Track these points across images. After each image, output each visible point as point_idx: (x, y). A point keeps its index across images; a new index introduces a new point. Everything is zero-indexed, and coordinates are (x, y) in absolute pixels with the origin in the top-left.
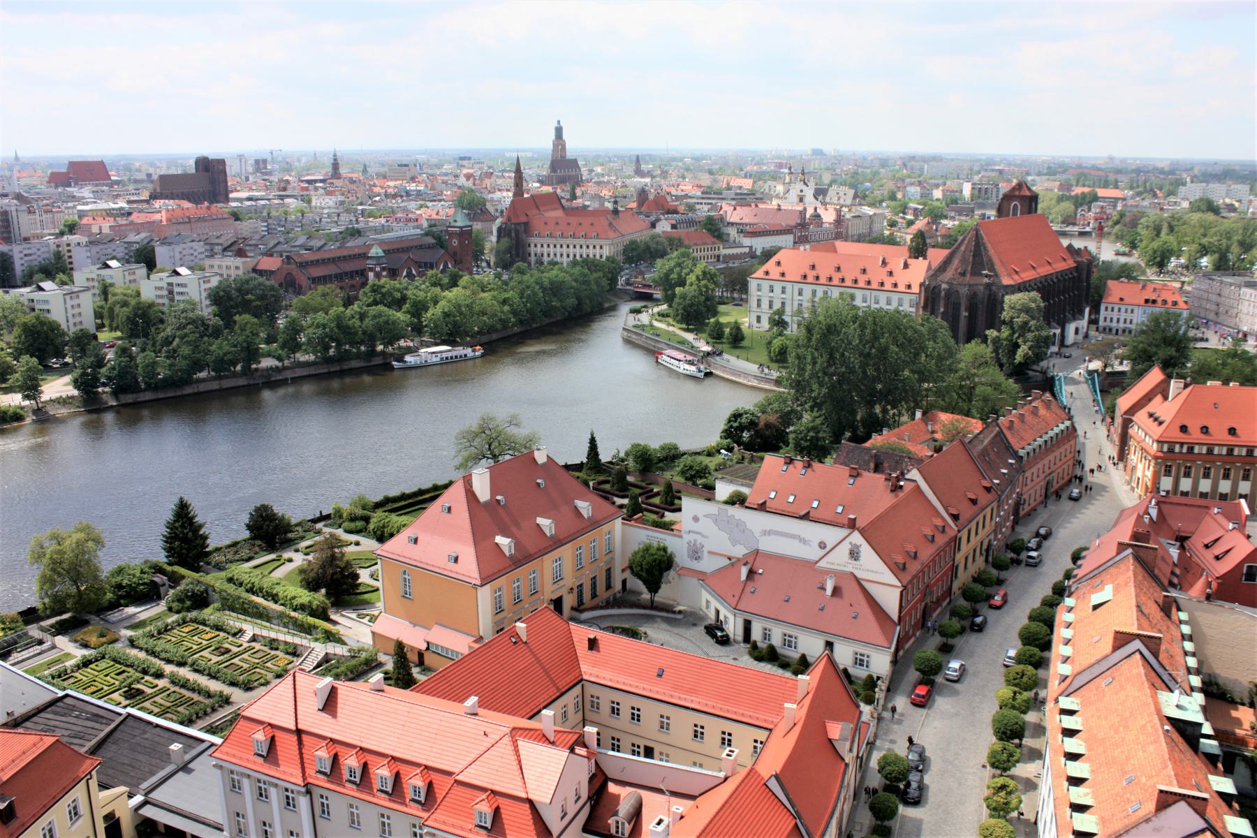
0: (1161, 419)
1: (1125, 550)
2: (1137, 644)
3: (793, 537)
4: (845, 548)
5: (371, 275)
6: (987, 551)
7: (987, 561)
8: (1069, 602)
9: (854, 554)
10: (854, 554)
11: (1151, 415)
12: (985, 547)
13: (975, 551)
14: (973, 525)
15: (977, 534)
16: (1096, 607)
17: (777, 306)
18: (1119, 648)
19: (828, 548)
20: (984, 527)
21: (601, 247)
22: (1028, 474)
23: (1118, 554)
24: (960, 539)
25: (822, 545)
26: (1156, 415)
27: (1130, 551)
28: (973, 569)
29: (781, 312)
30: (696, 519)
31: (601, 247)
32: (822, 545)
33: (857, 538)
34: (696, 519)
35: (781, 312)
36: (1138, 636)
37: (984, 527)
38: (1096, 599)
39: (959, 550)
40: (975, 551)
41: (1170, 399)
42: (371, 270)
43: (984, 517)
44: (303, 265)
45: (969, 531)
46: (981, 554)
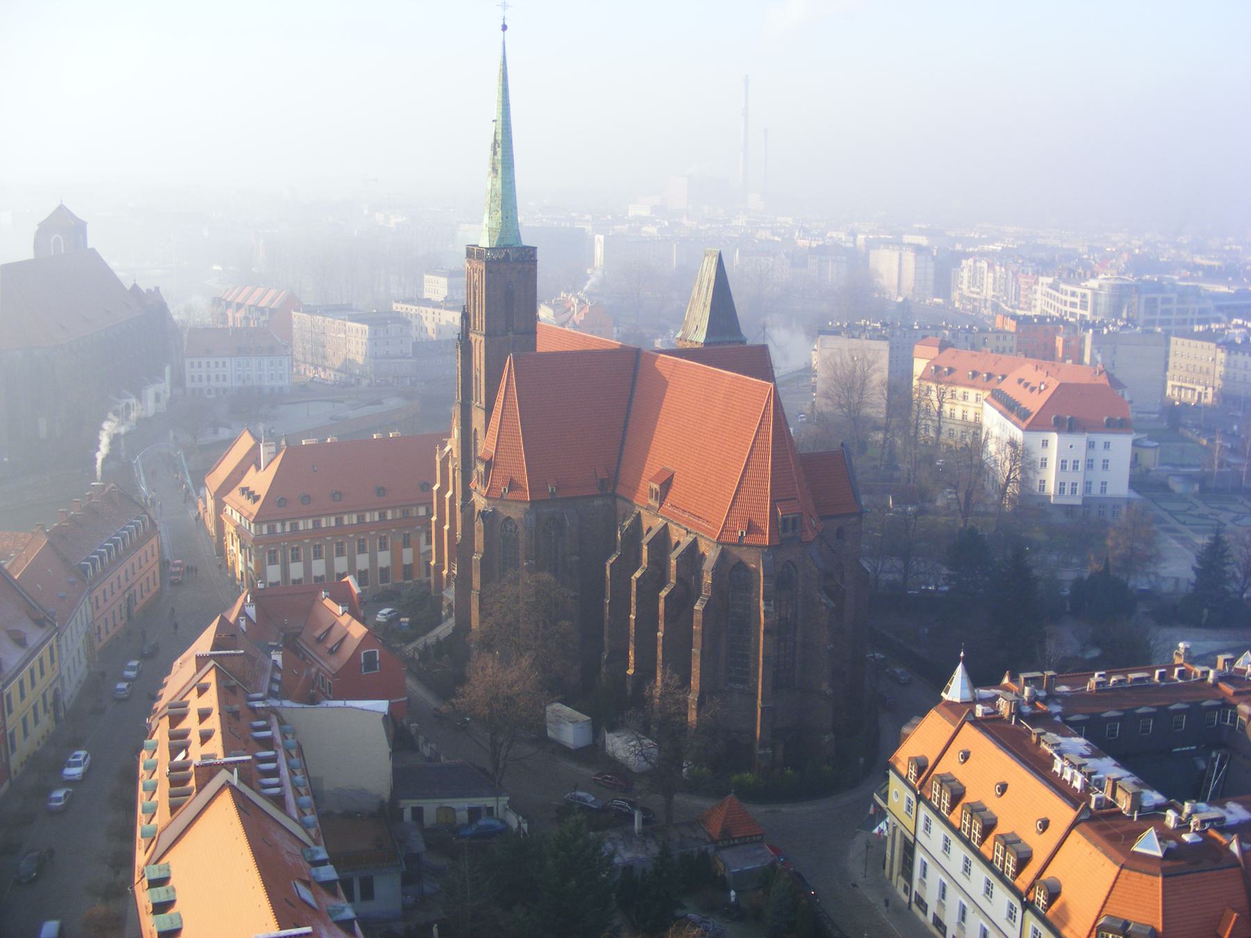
0: (256, 494)
1: (206, 663)
2: (223, 776)
7: (57, 719)
11: (245, 491)
12: (49, 700)
13: (35, 708)
14: (25, 672)
15: (33, 684)
18: (204, 786)
20: (42, 674)
22: (98, 592)
23: (198, 670)
24: (9, 697)
26: (251, 490)
27: (212, 663)
28: (37, 732)
36: (228, 766)
37: (42, 674)
39: (10, 711)
40: (35, 708)
41: (262, 469)
43: (41, 660)
45: (21, 683)
46: (46, 711)
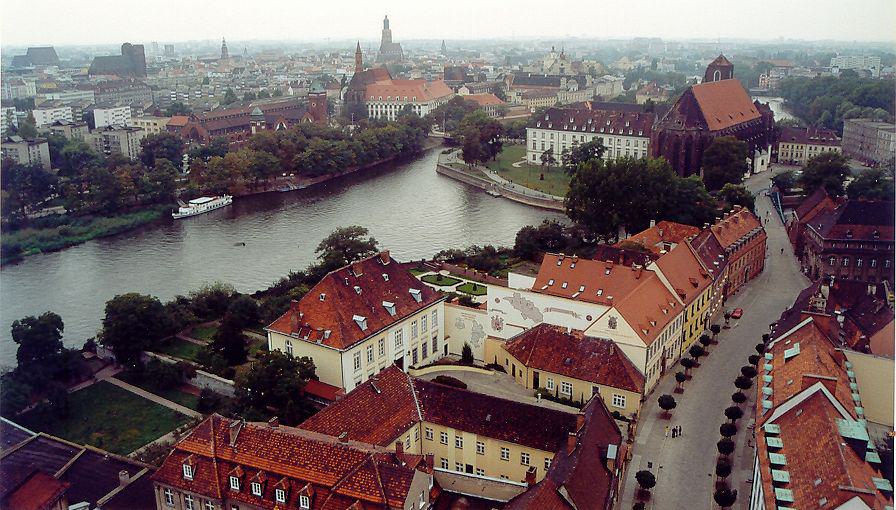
3: (567, 312)
4: (606, 319)
5: (253, 128)
6: (706, 320)
8: (768, 356)
9: (612, 324)
10: (612, 324)
16: (788, 360)
17: (547, 148)
19: (593, 321)
21: (419, 107)
25: (589, 318)
29: (550, 152)
30: (497, 301)
31: (419, 107)
32: (589, 318)
33: (614, 312)
34: (497, 301)
35: (550, 152)
36: (820, 379)
38: (788, 353)
42: (254, 125)
44: (203, 122)
